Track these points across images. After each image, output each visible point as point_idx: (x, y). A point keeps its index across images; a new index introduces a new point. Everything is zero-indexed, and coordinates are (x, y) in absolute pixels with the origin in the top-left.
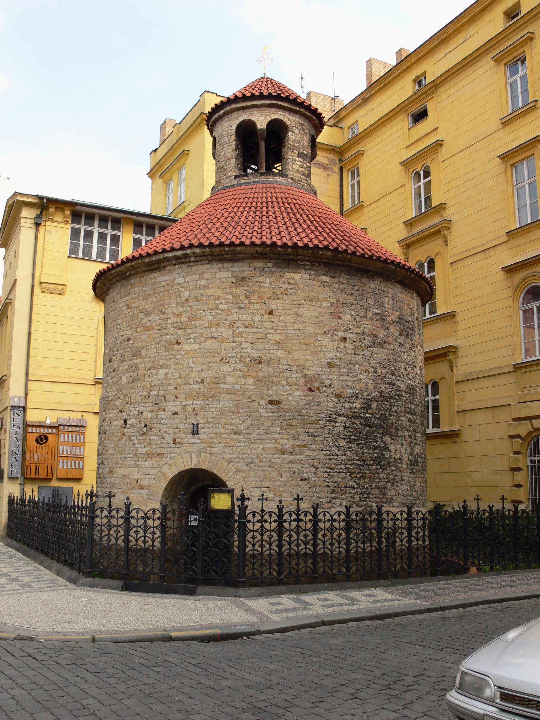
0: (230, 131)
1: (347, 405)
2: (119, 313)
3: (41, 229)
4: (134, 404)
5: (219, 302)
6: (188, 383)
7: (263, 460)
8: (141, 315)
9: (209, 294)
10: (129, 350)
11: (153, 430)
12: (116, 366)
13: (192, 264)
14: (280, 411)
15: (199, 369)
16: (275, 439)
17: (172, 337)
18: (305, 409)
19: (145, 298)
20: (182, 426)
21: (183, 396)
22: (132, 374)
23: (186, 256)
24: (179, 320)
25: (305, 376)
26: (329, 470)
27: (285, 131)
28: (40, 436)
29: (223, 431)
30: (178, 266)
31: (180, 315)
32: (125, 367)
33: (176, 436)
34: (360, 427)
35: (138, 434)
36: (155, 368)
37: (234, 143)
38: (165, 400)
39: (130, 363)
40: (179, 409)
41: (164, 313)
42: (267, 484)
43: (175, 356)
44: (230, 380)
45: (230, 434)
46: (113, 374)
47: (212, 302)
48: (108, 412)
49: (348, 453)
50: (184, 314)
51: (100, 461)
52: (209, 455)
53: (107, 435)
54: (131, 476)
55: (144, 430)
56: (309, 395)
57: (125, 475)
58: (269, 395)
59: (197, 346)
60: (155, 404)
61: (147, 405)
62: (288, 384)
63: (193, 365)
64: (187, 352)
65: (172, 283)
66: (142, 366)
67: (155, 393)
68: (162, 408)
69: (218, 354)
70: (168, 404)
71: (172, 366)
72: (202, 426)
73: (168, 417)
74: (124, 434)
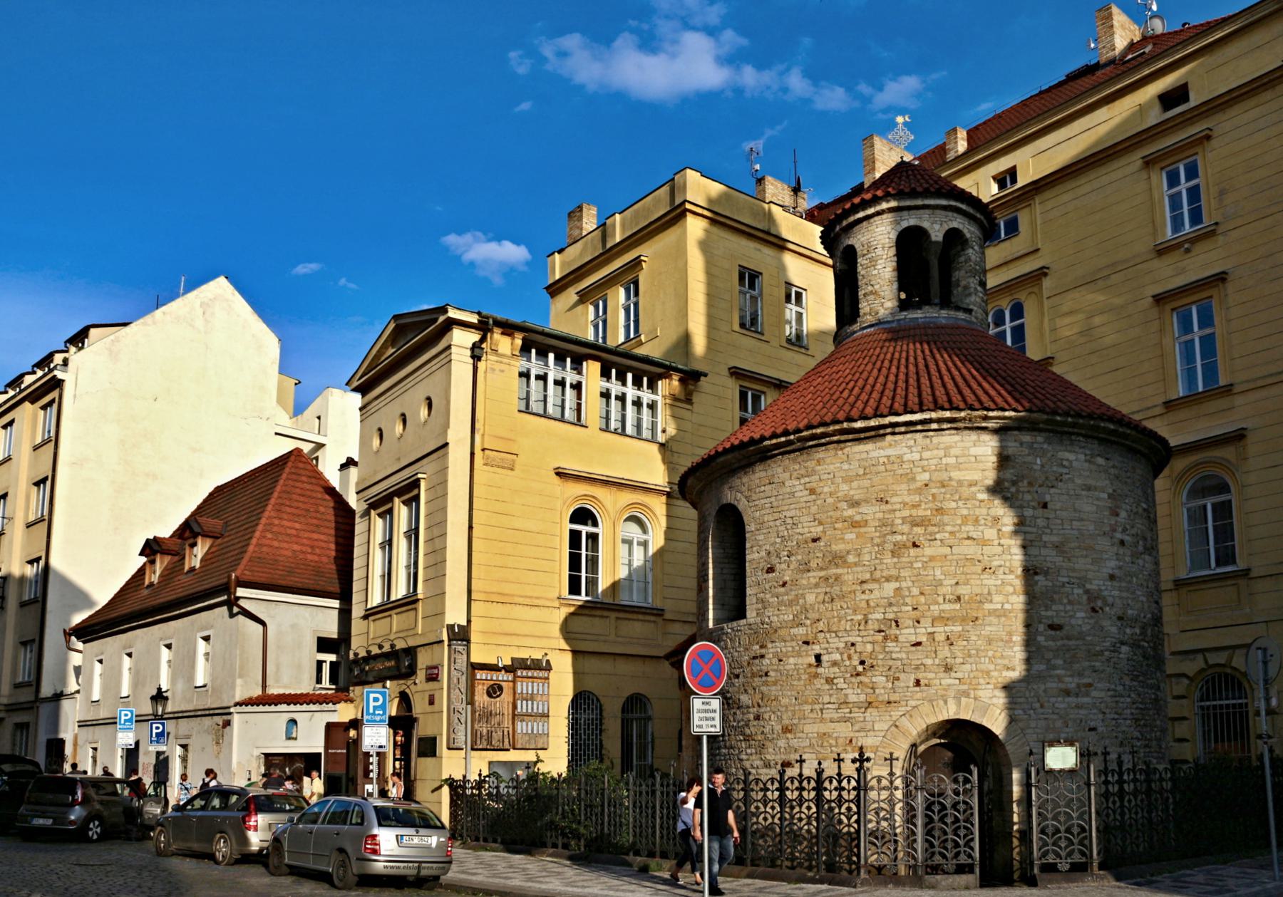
1: (1128, 631)
2: (789, 501)
4: (835, 632)
7: (1046, 704)
8: (844, 505)
10: (818, 555)
12: (787, 578)
13: (931, 433)
14: (1062, 639)
15: (954, 582)
17: (905, 537)
18: (1089, 635)
19: (848, 480)
20: (929, 662)
21: (930, 620)
22: (828, 590)
24: (914, 512)
26: (1116, 716)
27: (959, 248)
28: (492, 686)
29: (992, 667)
30: (909, 436)
32: (813, 581)
33: (920, 676)
34: (1141, 659)
37: (895, 259)
38: (898, 626)
39: (823, 573)
40: (923, 639)
41: (887, 502)
43: (912, 563)
44: (997, 598)
45: (1000, 671)
46: (782, 590)
49: (1133, 695)
50: (923, 505)
55: (860, 668)
56: (1092, 617)
58: (1047, 617)
59: (947, 550)
60: (880, 631)
61: (863, 633)
62: (1070, 602)
63: (943, 577)
64: (932, 559)
67: (880, 616)
69: (979, 561)
72: (961, 660)
73: (904, 649)
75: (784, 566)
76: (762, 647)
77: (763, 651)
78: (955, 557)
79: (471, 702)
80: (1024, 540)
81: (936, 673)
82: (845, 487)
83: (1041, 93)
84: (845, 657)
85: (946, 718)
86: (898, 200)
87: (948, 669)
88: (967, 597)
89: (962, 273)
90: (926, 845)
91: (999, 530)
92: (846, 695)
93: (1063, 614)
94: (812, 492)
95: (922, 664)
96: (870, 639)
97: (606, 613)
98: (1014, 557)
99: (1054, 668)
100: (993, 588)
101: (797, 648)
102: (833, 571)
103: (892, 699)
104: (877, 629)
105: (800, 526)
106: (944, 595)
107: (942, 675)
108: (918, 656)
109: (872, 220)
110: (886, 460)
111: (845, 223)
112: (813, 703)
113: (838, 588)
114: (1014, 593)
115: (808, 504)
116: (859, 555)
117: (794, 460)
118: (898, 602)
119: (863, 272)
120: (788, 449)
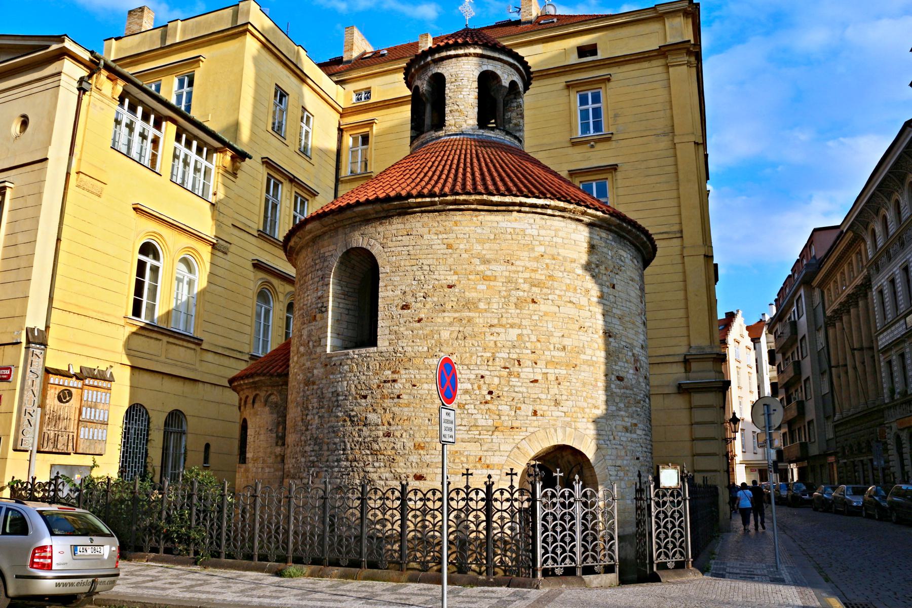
0: (472, 76)
3: (85, 98)
4: (467, 365)
5: (576, 265)
7: (616, 437)
8: (477, 261)
9: (566, 255)
10: (453, 299)
11: (502, 398)
12: (422, 316)
13: (546, 217)
15: (561, 334)
16: (622, 416)
17: (526, 293)
20: (543, 396)
22: (461, 329)
23: (543, 207)
24: (533, 275)
25: (633, 355)
27: (513, 96)
29: (585, 405)
30: (530, 215)
33: (537, 408)
35: (479, 402)
36: (502, 326)
37: (477, 90)
38: (520, 365)
39: (457, 315)
40: (539, 377)
41: (512, 264)
42: (619, 463)
44: (589, 352)
46: (418, 325)
48: (403, 372)
51: (381, 434)
52: (573, 430)
53: (401, 401)
54: (466, 453)
55: (488, 397)
56: (635, 374)
57: (457, 452)
58: (616, 370)
60: (505, 368)
61: (491, 368)
62: (627, 362)
63: (553, 330)
64: (546, 314)
65: (522, 233)
67: (505, 356)
68: (516, 374)
69: (577, 321)
70: (524, 370)
71: (528, 327)
73: (524, 384)
75: (419, 305)
77: (396, 376)
78: (562, 315)
79: (42, 406)
80: (604, 309)
81: (549, 406)
82: (478, 247)
84: (475, 387)
85: (556, 444)
87: (557, 403)
88: (569, 348)
89: (514, 114)
90: (583, 549)
91: (589, 299)
92: (476, 419)
93: (623, 369)
95: (538, 398)
96: (497, 373)
97: (159, 337)
98: (598, 321)
99: (619, 410)
100: (586, 343)
102: (466, 314)
103: (515, 425)
104: (503, 366)
106: (554, 344)
107: (553, 408)
109: (460, 59)
111: (437, 56)
113: (470, 329)
114: (598, 349)
115: (445, 256)
116: (489, 303)
117: (433, 219)
118: (520, 345)
119: (450, 94)
120: (429, 208)
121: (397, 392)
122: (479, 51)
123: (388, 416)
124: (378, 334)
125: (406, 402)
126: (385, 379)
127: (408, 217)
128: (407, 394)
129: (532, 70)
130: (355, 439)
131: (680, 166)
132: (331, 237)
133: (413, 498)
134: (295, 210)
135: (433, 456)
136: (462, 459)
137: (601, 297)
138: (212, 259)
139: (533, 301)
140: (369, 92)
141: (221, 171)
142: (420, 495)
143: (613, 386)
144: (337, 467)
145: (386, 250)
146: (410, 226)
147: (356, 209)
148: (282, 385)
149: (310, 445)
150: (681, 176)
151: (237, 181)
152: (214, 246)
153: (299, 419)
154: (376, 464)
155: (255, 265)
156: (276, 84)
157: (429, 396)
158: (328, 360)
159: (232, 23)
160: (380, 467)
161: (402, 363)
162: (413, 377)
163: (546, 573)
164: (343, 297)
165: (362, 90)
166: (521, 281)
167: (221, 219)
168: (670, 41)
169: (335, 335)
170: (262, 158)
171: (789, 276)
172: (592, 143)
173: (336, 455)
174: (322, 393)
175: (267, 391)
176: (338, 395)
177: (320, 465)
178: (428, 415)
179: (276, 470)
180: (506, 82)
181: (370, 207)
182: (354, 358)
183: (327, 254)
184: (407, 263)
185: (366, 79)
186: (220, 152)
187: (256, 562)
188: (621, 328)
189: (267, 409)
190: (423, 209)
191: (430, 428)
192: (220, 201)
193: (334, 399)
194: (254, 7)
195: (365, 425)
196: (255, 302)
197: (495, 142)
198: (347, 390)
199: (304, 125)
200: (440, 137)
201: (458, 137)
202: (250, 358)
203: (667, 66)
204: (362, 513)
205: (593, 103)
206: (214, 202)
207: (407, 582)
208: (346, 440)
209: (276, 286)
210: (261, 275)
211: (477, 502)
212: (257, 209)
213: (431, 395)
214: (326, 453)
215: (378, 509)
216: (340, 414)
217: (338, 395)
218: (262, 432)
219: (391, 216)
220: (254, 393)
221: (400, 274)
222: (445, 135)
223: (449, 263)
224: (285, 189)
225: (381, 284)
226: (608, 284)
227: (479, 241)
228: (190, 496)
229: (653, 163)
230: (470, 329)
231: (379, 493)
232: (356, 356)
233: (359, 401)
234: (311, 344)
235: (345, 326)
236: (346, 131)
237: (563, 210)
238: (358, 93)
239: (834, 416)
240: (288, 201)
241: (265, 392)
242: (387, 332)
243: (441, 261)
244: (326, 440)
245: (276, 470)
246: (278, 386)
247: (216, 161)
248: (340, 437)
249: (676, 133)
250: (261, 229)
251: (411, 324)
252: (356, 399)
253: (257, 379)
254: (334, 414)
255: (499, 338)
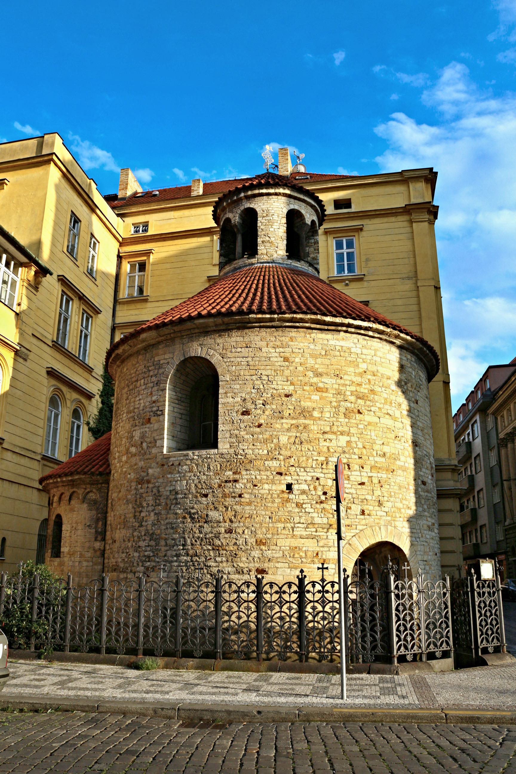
2: (265, 363)
4: (304, 468)
6: (373, 456)
8: (310, 374)
10: (290, 407)
12: (262, 421)
13: (367, 338)
17: (353, 405)
19: (314, 356)
20: (369, 497)
22: (298, 435)
23: (367, 329)
31: (359, 385)
33: (365, 508)
35: (315, 502)
36: (334, 433)
37: (286, 225)
38: (349, 468)
39: (294, 422)
40: (365, 480)
41: (341, 378)
44: (402, 458)
46: (258, 430)
47: (385, 380)
48: (244, 473)
51: (223, 530)
53: (242, 500)
54: (304, 549)
55: (323, 498)
57: (296, 548)
59: (376, 420)
61: (325, 471)
63: (375, 438)
64: (369, 424)
65: (348, 351)
66: (314, 428)
70: (353, 473)
73: (354, 486)
74: (288, 500)
75: (259, 411)
76: (234, 473)
77: (237, 477)
81: (374, 506)
83: (235, 180)
84: (312, 487)
85: (380, 540)
86: (292, 190)
89: (312, 249)
94: (286, 359)
100: (400, 451)
101: (272, 477)
102: (302, 421)
105: (274, 383)
107: (377, 508)
108: (363, 492)
109: (271, 197)
110: (340, 348)
111: (250, 193)
112: (285, 522)
113: (306, 435)
114: (409, 456)
115: (282, 368)
116: (322, 412)
117: (271, 334)
118: (349, 451)
119: (262, 227)
120: (268, 324)
121: (238, 491)
122: (287, 191)
123: (230, 514)
124: (219, 437)
125: (248, 500)
126: (226, 479)
127: (247, 331)
128: (248, 493)
129: (326, 213)
130: (196, 535)
131: (422, 305)
132: (167, 346)
133: (269, 591)
134: (82, 326)
135: (274, 552)
136: (301, 554)
137: (409, 411)
138: (14, 364)
139: (359, 412)
140: (147, 226)
141: (25, 284)
142: (276, 588)
143: (420, 490)
144: (176, 561)
145: (225, 360)
146: (249, 339)
147: (196, 322)
148: (102, 483)
149: (145, 540)
150: (423, 314)
151: (38, 294)
152: (16, 352)
153: (131, 515)
154: (219, 559)
155: (49, 373)
156: (72, 211)
157: (270, 496)
158: (165, 460)
159: (36, 153)
160: (222, 562)
161: (243, 464)
162: (254, 477)
163: (402, 659)
164: (177, 402)
165: (140, 223)
166: (348, 393)
167: (24, 328)
168: (414, 201)
169: (171, 437)
170: (58, 276)
171: (464, 405)
172: (347, 282)
173: (175, 550)
174: (159, 491)
175: (85, 489)
176: (177, 493)
177: (157, 560)
178: (268, 513)
179: (95, 564)
180: (308, 221)
181: (211, 320)
182: (193, 459)
183: (162, 362)
184: (247, 373)
185: (144, 214)
186: (25, 267)
187: (103, 655)
188: (423, 439)
189: (85, 506)
190: (262, 324)
191: (271, 525)
192: (24, 311)
193: (174, 497)
194: (58, 141)
195: (206, 522)
196: (48, 407)
197: (300, 271)
198: (187, 489)
199: (91, 250)
200: (253, 264)
201: (271, 265)
202: (42, 459)
203: (411, 222)
204: (216, 606)
205: (347, 248)
206: (18, 312)
207: (266, 671)
208: (186, 536)
209: (65, 393)
210: (53, 382)
211: (290, 595)
212: (53, 321)
213: (272, 495)
214: (163, 549)
215: (233, 601)
216: (179, 511)
217: (177, 493)
218: (80, 527)
219: (230, 330)
220: (71, 491)
221: (240, 382)
222: (258, 263)
223: (286, 374)
224: (75, 306)
225: (221, 391)
226: (413, 399)
227: (312, 356)
228: (31, 591)
229: (399, 302)
230: (306, 435)
231: (234, 587)
232: (195, 457)
233: (200, 499)
234: (144, 445)
235: (178, 430)
236: (125, 258)
237: (382, 332)
238: (136, 226)
239: (505, 521)
240: (77, 317)
241: (83, 490)
242: (228, 435)
243: (278, 372)
244: (163, 536)
245: (95, 564)
246: (97, 484)
247: (21, 275)
248: (179, 534)
249: (419, 278)
250: (55, 340)
251: (252, 429)
252: (196, 497)
253: (76, 477)
254: (172, 512)
255: (331, 444)
